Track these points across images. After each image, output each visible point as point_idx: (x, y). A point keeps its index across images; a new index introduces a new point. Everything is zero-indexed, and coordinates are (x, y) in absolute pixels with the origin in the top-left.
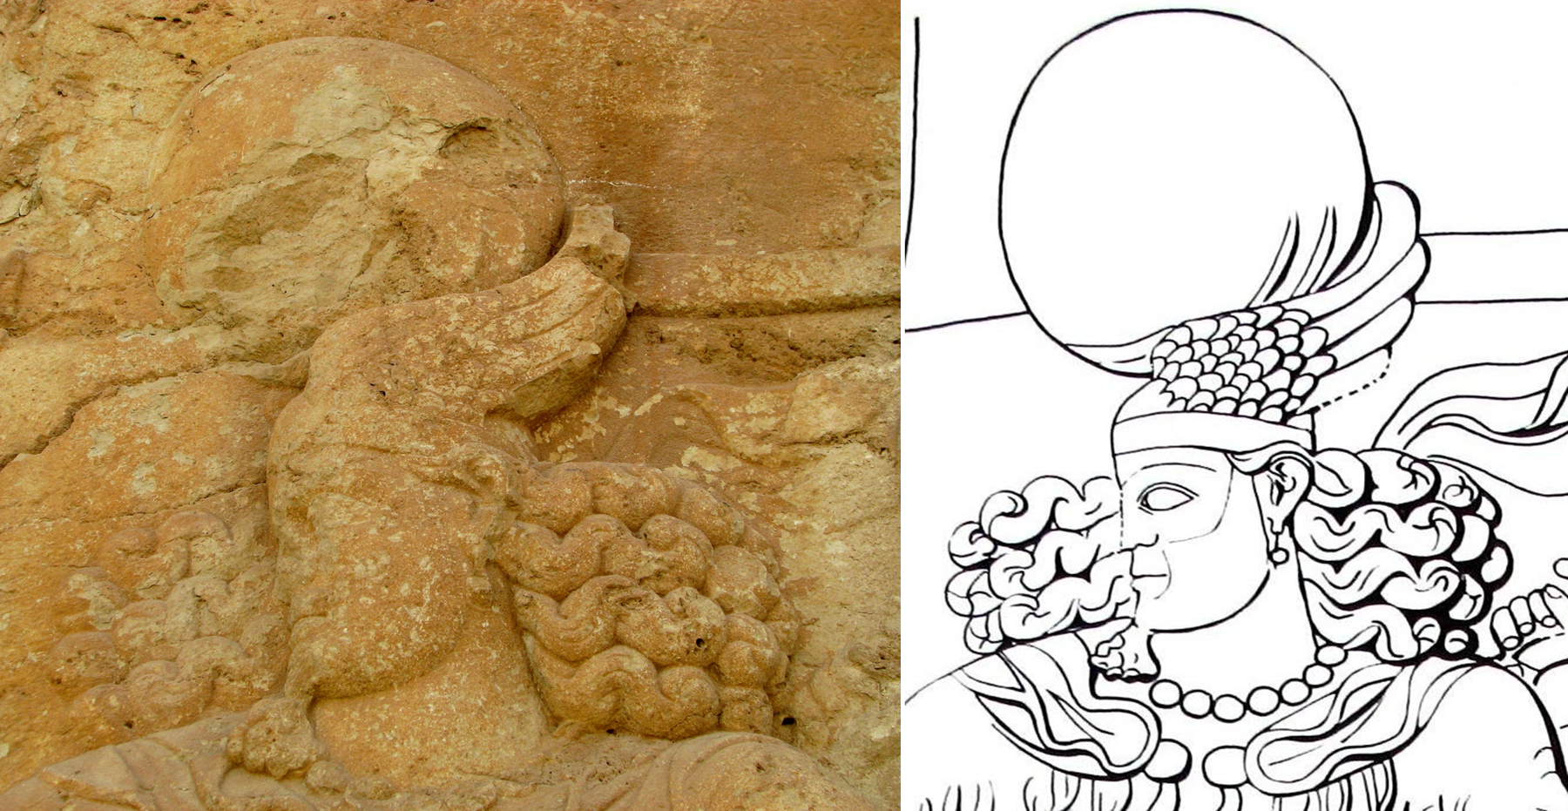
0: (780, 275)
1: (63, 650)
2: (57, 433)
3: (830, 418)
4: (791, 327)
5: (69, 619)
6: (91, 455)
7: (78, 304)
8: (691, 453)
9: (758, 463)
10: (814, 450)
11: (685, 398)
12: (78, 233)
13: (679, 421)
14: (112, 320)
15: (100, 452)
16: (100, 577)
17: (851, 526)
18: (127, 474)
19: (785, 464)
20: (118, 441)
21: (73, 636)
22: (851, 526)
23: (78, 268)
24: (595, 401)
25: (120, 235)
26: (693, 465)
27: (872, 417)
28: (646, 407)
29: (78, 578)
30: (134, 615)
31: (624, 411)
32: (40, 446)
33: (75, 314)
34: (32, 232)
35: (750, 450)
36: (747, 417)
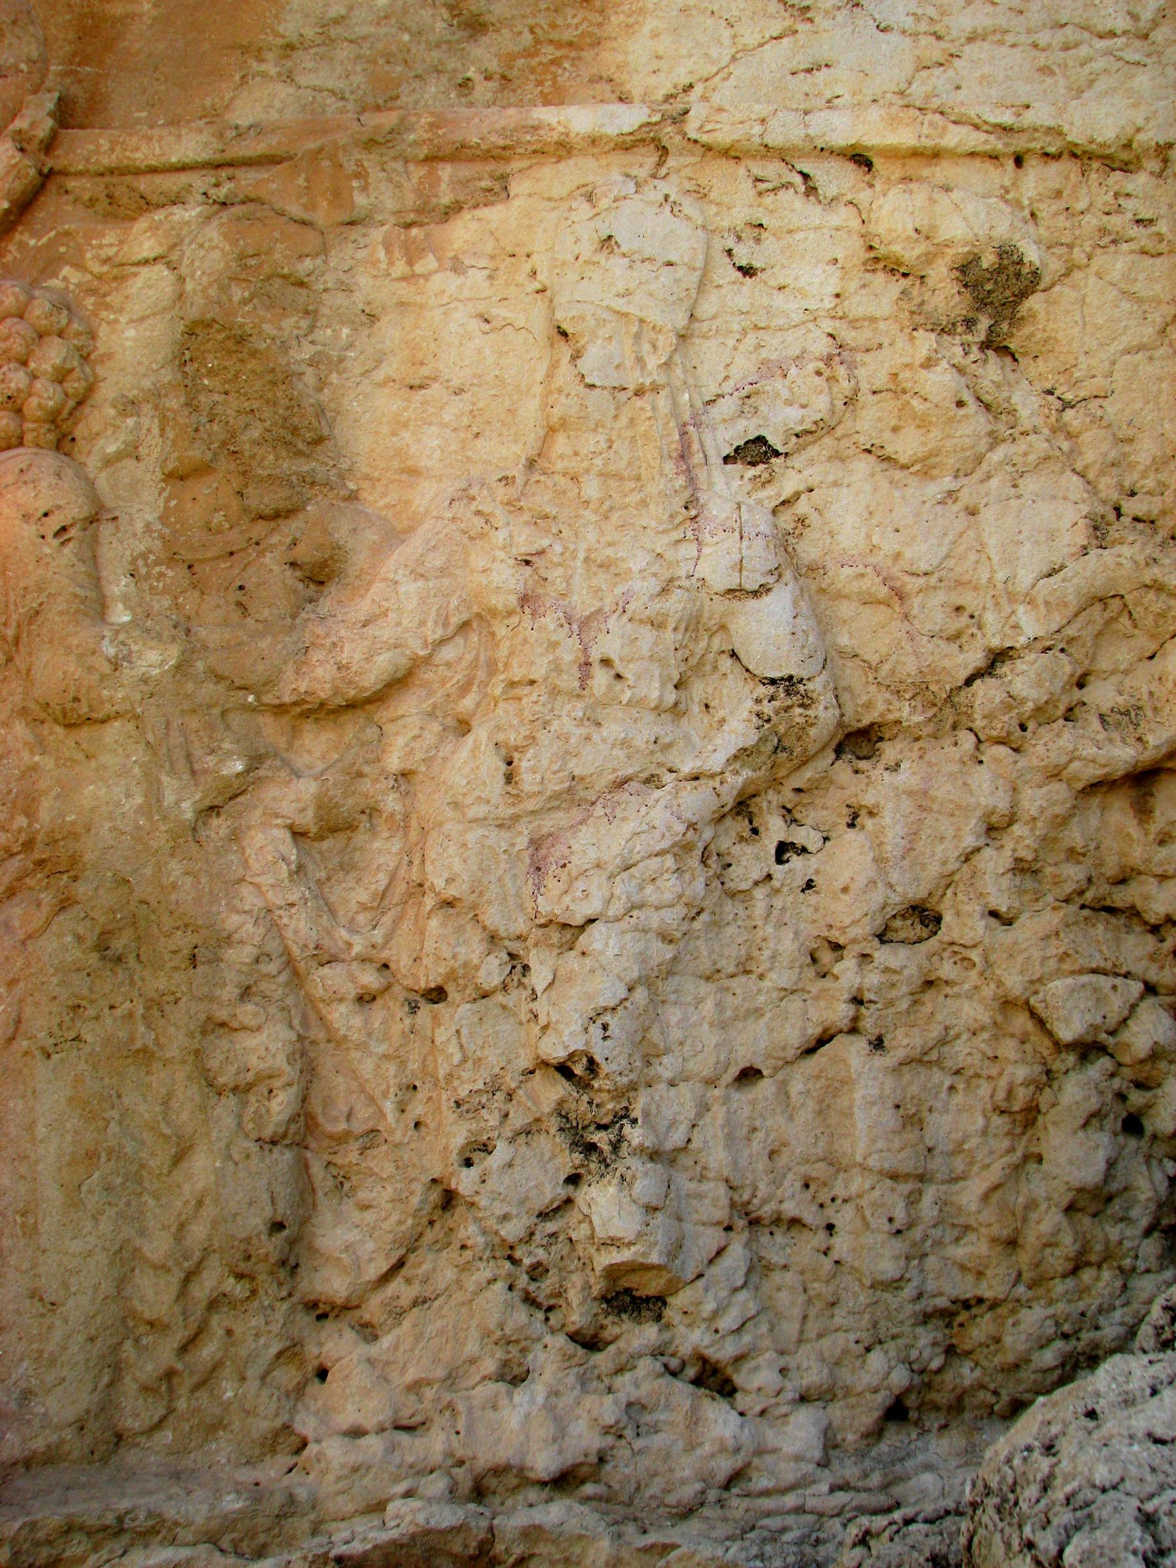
0: (144, 147)
3: (147, 247)
4: (144, 184)
8: (66, 271)
9: (99, 277)
10: (134, 269)
11: (67, 234)
13: (62, 249)
17: (143, 319)
19: (115, 278)
22: (143, 319)
24: (17, 237)
26: (65, 279)
27: (175, 246)
28: (45, 239)
31: (32, 242)
35: (97, 268)
36: (101, 246)
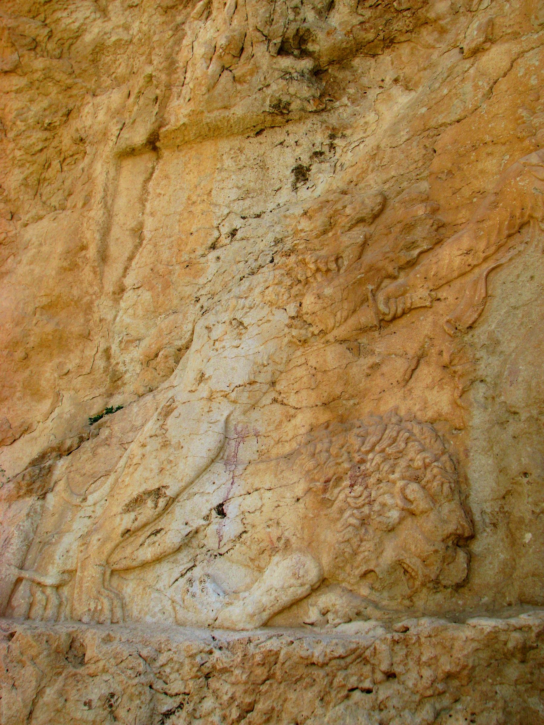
1: (519, 130)
2: (509, 71)
5: (519, 121)
6: (519, 75)
7: (509, 31)
12: (506, 8)
14: (519, 33)
15: (521, 74)
16: (526, 109)
18: (530, 78)
20: (526, 70)
21: (521, 125)
23: (508, 19)
25: (518, 6)
29: (520, 110)
30: (537, 117)
32: (505, 75)
33: (509, 34)
34: (493, 10)
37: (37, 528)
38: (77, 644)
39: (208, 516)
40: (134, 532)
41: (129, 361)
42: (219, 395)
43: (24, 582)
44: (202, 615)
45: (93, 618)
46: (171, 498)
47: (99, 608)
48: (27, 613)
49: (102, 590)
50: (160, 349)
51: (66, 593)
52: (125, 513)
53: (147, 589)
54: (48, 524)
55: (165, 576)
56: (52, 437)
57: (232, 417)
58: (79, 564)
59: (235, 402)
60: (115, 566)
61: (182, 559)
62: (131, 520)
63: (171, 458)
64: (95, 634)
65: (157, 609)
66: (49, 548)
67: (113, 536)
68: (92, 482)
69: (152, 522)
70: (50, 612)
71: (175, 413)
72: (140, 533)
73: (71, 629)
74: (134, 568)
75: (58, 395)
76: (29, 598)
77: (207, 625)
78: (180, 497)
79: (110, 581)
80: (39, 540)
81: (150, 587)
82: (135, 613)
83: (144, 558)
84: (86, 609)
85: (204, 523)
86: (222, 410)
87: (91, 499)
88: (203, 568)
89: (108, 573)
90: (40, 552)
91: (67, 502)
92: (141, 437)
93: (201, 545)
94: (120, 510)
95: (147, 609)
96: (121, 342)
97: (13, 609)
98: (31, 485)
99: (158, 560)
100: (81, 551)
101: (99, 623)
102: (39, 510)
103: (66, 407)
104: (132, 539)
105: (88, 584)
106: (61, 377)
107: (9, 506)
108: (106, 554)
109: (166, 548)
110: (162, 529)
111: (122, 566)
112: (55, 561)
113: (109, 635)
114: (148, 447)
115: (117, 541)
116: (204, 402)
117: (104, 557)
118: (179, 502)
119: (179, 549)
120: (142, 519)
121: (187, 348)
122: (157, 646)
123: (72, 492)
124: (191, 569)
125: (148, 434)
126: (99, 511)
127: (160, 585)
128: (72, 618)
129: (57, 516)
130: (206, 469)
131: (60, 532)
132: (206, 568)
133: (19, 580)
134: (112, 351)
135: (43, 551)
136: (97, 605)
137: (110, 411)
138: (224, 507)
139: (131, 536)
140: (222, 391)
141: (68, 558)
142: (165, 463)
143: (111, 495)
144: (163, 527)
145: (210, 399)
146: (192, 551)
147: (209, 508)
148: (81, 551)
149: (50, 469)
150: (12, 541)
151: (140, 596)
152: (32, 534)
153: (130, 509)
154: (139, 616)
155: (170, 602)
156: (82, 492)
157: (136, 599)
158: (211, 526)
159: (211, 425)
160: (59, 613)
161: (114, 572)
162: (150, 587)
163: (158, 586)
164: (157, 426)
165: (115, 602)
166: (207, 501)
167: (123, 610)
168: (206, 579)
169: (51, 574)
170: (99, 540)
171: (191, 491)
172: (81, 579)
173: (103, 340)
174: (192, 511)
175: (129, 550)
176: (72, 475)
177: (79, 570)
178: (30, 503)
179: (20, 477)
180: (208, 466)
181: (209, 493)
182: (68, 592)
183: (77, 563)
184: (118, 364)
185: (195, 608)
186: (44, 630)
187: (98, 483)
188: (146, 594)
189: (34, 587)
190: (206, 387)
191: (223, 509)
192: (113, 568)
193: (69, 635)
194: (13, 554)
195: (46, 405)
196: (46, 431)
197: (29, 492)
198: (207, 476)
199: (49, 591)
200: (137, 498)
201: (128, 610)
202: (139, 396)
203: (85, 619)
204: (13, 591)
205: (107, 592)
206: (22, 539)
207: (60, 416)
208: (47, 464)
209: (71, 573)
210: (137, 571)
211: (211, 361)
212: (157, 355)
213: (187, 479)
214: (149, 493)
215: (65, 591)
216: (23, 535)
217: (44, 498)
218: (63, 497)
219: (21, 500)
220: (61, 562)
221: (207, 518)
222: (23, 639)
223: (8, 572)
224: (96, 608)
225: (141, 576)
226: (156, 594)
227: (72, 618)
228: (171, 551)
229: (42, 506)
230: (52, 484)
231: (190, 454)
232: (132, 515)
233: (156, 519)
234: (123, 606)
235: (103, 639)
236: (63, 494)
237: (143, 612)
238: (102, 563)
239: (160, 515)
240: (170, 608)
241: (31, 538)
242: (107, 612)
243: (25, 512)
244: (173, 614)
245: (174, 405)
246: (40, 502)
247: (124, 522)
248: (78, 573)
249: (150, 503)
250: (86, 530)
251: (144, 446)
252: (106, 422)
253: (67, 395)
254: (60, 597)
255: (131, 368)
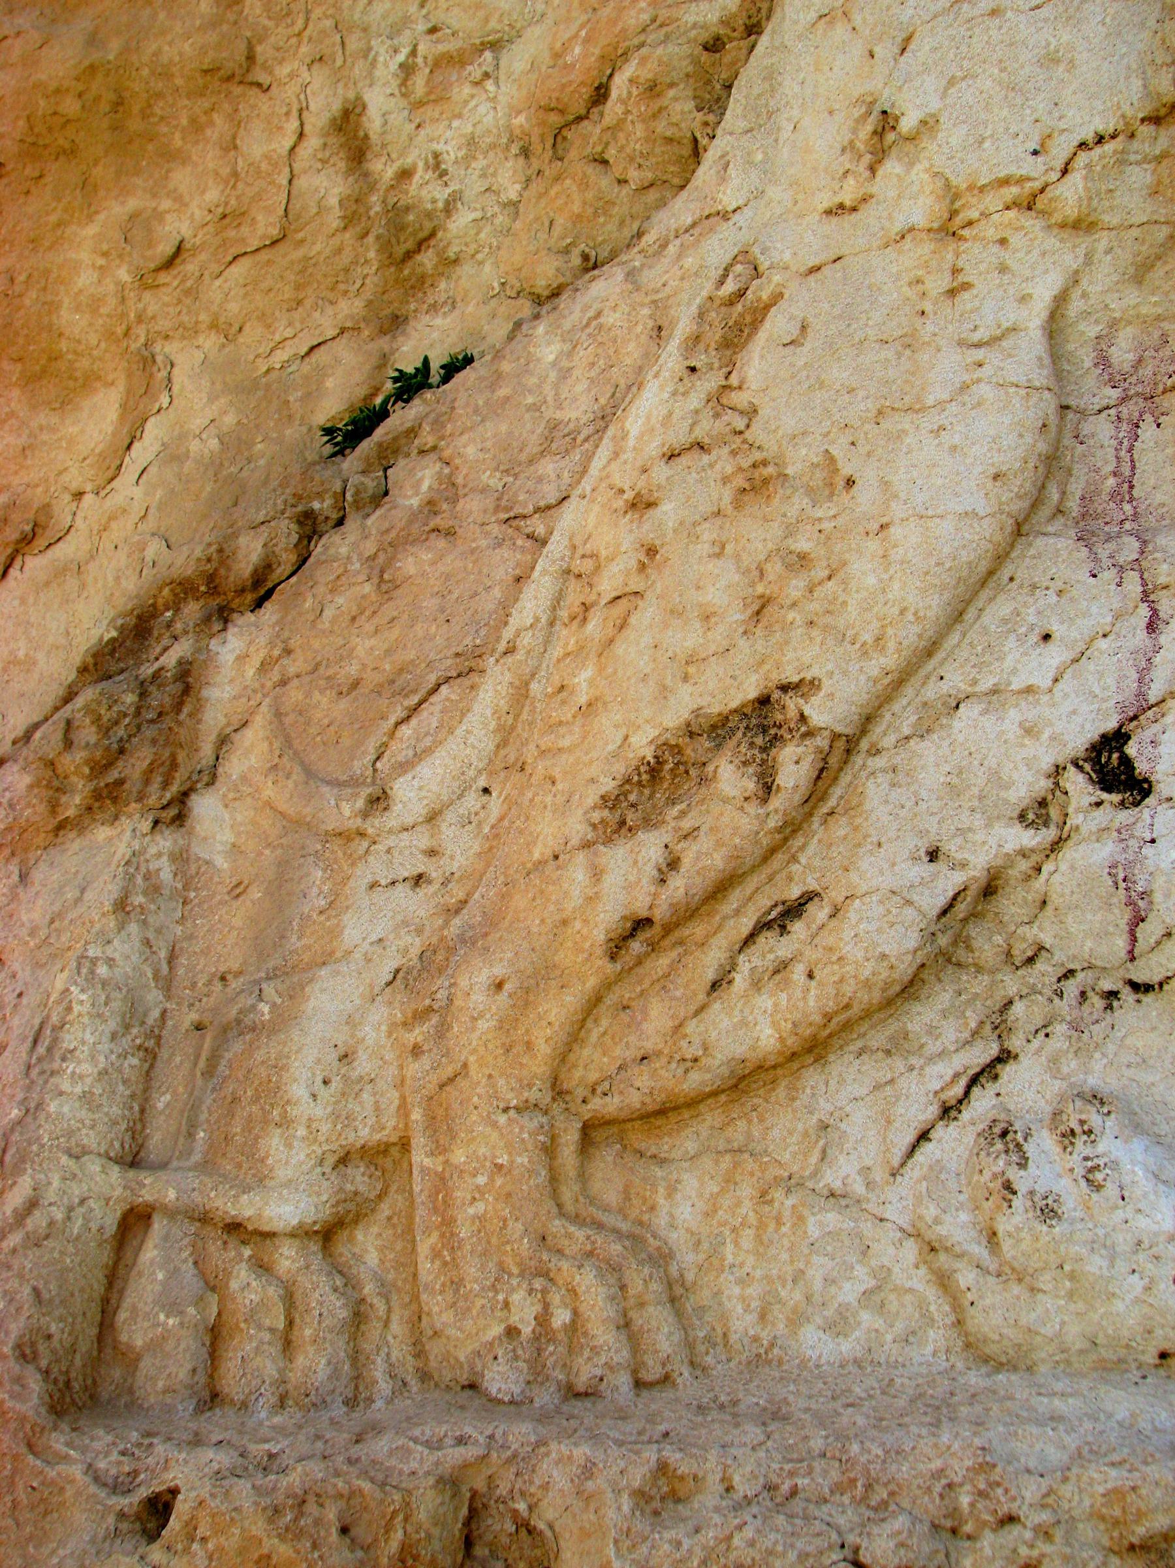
37: (172, 959)
38: (498, 1526)
39: (1043, 803)
40: (668, 929)
41: (462, 152)
42: (993, 201)
43: (158, 1224)
44: (1119, 1306)
45: (537, 1373)
46: (835, 736)
47: (561, 1317)
48: (201, 1378)
49: (557, 1226)
50: (614, 60)
51: (372, 1258)
52: (608, 841)
53: (778, 1194)
54: (223, 937)
55: (858, 1123)
56: (154, 548)
57: (1075, 306)
58: (416, 1115)
59: (1081, 225)
60: (596, 1103)
61: (932, 1031)
62: (650, 871)
63: (802, 544)
64: (588, 1470)
65: (849, 1292)
66: (251, 1048)
67: (565, 957)
68: (398, 713)
69: (754, 869)
70: (315, 1363)
71: (777, 324)
72: (696, 929)
73: (455, 1455)
74: (694, 1102)
75: (147, 361)
76: (199, 1301)
77: (1151, 1358)
78: (877, 730)
79: (583, 1177)
80: (194, 1016)
81: (791, 1183)
82: (742, 1323)
83: (740, 1050)
84: (497, 1330)
85: (1029, 838)
86: (1024, 275)
87: (410, 795)
88: (1054, 1061)
89: (570, 1138)
90: (209, 1073)
91: (295, 824)
92: (612, 467)
93: (1021, 950)
94: (576, 828)
95: (798, 1296)
96: (407, 69)
97: (130, 1360)
98: (110, 765)
99: (812, 1049)
100: (416, 1051)
101: (572, 1393)
102: (166, 875)
103: (195, 409)
104: (663, 962)
105: (480, 1207)
106: (145, 282)
107: (24, 877)
108: (543, 1049)
109: (848, 989)
110: (809, 897)
111: (635, 1100)
112: (293, 1112)
113: (663, 1468)
114: (666, 507)
115: (592, 982)
116: (920, 250)
117: (538, 1065)
118: (875, 751)
119: (910, 989)
120: (704, 859)
121: (753, 30)
122: (931, 1506)
123: (309, 773)
124: (988, 1072)
125: (654, 448)
126: (460, 848)
127: (842, 1171)
128: (425, 1376)
129: (256, 893)
130: (991, 573)
131: (285, 965)
132: (1070, 1065)
133: (135, 1220)
134: (373, 123)
135: (222, 1068)
136: (546, 1306)
137: (411, 386)
138: (1131, 750)
139: (654, 947)
140: (1005, 182)
141: (353, 1087)
142: (774, 569)
143: (508, 762)
144: (813, 886)
145: (949, 229)
146: (978, 985)
147: (1046, 762)
148: (416, 1051)
149: (187, 681)
150: (69, 1040)
151: (750, 1232)
152: (154, 996)
153: (631, 818)
154: (765, 1336)
155: (910, 1250)
156: (361, 765)
157: (729, 1250)
158: (1069, 853)
159: (979, 354)
160: (356, 1356)
161: (601, 1132)
162: (791, 1183)
163: (831, 1178)
164: (695, 401)
165: (637, 1278)
166: (1029, 731)
167: (679, 1314)
168: (1095, 1119)
169: (282, 1174)
170: (499, 986)
171: (932, 691)
172: (441, 1182)
173: (318, 79)
174: (953, 791)
175: (657, 1017)
176: (294, 694)
177: (419, 1142)
178: (122, 850)
179: (48, 739)
180: (1001, 558)
181: (1029, 690)
182: (381, 1249)
183: (403, 1109)
184: (405, 174)
185: (1072, 1277)
186: (317, 1470)
187: (430, 716)
188: (779, 1222)
189: (213, 1248)
190: (919, 173)
191: (1126, 762)
192: (587, 1111)
193: (450, 1483)
194: (86, 1098)
195: (98, 418)
196: (118, 530)
197: (108, 798)
198: (1003, 607)
199: (287, 1258)
200: (659, 761)
201: (701, 1310)
202: (538, 301)
203: (501, 1379)
204: (115, 1277)
205: (580, 1234)
206: (112, 1025)
207: (172, 454)
208: (170, 659)
209: (385, 1157)
210: (711, 1117)
211: (922, 48)
212: (601, 94)
213: (909, 635)
214: (718, 729)
215: (368, 1247)
216: (115, 1005)
217: (180, 819)
218: (269, 804)
219: (74, 844)
220: (319, 1112)
221: (1037, 813)
222: (219, 1530)
223: (76, 1191)
224: (543, 1319)
225: (738, 1133)
226: (832, 1218)
227: (425, 1376)
228: (876, 996)
229: (181, 858)
230: (207, 750)
231: (897, 510)
232: (650, 847)
233: (773, 851)
234: (675, 1295)
235: (641, 1496)
236: (269, 791)
237: (779, 1316)
238: (533, 1095)
239: (791, 829)
240: (919, 1281)
241: (156, 1013)
242: (603, 1335)
243: (105, 890)
244: (939, 1307)
245: (761, 291)
246: (166, 841)
247: (612, 881)
248: (420, 1157)
249: (730, 777)
250: (416, 945)
251: (641, 504)
252: (412, 432)
253: (187, 361)
254: (345, 1279)
255: (473, 185)
